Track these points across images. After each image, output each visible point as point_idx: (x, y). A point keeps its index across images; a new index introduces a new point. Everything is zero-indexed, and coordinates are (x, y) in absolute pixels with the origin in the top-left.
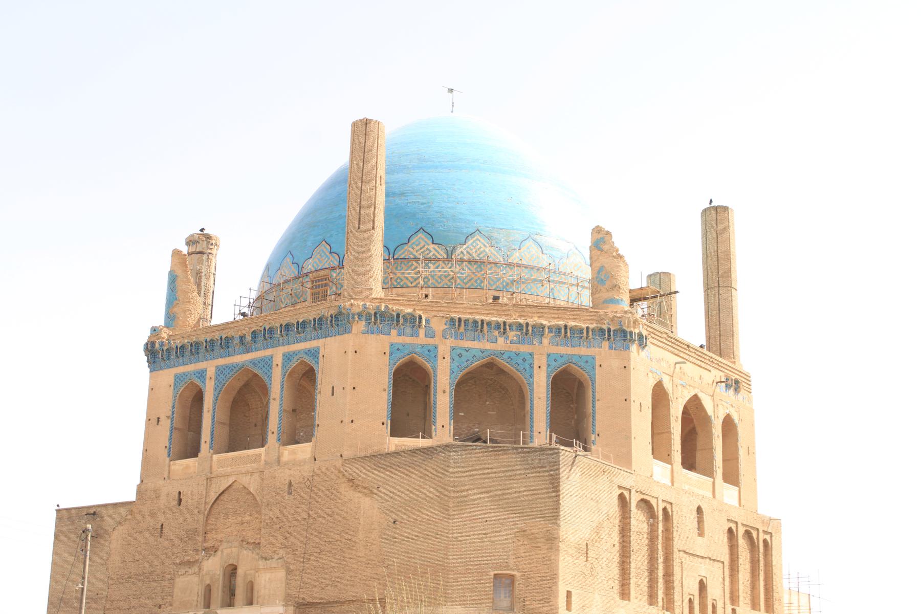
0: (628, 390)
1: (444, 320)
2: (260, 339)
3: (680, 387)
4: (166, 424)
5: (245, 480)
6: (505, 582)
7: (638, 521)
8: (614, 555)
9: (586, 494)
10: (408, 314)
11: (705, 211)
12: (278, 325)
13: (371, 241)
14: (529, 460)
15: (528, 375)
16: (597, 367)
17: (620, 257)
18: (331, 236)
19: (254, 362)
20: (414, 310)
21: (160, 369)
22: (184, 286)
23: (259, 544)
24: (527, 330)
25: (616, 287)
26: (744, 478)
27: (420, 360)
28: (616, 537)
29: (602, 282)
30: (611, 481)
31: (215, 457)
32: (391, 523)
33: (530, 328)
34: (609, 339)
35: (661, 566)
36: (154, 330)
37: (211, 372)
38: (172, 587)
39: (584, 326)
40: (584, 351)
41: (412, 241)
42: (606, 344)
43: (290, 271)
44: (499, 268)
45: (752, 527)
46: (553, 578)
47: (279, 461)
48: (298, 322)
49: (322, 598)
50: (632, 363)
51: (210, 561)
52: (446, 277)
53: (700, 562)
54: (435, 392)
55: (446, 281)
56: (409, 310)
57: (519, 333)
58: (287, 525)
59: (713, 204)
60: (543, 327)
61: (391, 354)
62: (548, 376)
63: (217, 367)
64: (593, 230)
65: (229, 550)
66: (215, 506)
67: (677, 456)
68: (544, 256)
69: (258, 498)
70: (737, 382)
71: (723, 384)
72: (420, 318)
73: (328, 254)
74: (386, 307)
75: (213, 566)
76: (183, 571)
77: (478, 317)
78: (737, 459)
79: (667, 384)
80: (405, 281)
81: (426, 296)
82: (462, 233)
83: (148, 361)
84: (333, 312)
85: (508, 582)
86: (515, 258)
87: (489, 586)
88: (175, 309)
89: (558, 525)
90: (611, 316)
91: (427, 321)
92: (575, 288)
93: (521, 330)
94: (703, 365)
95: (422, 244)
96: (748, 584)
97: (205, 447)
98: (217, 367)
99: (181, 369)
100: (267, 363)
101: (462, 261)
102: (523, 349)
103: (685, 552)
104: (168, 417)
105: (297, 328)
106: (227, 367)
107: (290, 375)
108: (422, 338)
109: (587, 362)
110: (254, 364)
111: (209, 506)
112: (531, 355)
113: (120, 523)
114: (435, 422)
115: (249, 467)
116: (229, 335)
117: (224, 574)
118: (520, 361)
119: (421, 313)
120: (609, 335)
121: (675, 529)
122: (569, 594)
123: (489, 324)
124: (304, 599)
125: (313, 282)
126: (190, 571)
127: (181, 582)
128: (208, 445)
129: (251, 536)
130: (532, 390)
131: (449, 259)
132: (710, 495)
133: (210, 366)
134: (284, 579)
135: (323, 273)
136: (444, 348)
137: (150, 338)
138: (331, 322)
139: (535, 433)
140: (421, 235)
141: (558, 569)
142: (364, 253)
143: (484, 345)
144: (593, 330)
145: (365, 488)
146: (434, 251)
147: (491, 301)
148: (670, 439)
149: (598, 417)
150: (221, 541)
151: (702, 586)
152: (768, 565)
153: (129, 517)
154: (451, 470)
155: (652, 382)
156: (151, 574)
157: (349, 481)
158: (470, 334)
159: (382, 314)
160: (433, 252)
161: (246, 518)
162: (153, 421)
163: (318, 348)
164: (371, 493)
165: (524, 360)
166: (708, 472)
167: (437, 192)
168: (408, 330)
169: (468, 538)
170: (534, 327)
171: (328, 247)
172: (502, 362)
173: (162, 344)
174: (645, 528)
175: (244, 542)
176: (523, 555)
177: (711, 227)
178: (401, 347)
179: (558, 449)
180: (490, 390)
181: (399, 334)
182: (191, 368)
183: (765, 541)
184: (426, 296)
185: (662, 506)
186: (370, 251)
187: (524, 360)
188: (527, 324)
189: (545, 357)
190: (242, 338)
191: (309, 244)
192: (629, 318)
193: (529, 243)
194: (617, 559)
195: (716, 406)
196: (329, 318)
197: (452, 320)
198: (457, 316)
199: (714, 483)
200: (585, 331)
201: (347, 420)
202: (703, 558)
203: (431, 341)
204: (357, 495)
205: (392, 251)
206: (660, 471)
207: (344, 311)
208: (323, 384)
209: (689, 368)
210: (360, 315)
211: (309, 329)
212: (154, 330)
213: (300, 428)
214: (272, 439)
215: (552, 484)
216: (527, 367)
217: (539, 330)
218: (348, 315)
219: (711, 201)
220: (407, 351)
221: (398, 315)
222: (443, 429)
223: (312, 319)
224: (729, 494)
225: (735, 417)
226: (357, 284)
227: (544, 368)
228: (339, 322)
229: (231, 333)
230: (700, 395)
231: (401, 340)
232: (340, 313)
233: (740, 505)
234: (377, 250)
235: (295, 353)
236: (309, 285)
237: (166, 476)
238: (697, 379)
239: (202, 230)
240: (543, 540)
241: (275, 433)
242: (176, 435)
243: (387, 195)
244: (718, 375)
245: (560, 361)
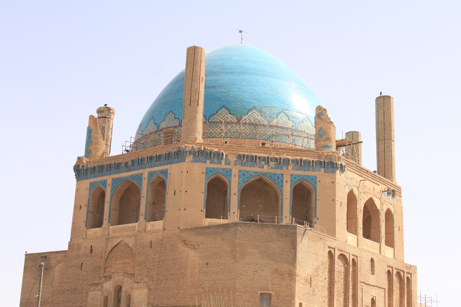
0: (334, 194)
1: (235, 156)
2: (136, 164)
3: (362, 194)
4: (85, 209)
5: (127, 240)
6: (266, 297)
7: (339, 266)
8: (326, 284)
9: (311, 251)
10: (216, 152)
11: (378, 98)
12: (146, 157)
13: (196, 112)
14: (280, 232)
15: (280, 186)
16: (318, 182)
17: (331, 123)
18: (175, 109)
19: (132, 177)
20: (219, 150)
21: (82, 180)
22: (96, 135)
23: (134, 274)
24: (280, 162)
25: (329, 139)
26: (397, 244)
27: (222, 177)
28: (326, 274)
29: (321, 136)
30: (324, 244)
31: (111, 227)
32: (205, 265)
33: (282, 160)
34: (324, 167)
35: (351, 290)
36: (79, 158)
37: (109, 182)
38: (87, 297)
39: (311, 160)
40: (310, 173)
41: (219, 113)
42: (322, 170)
43: (153, 128)
44: (265, 128)
45: (401, 270)
46: (292, 296)
47: (145, 230)
48: (156, 155)
49: (167, 304)
50: (337, 180)
51: (107, 283)
52: (237, 132)
53: (372, 287)
54: (230, 194)
55: (237, 134)
56: (216, 150)
57: (276, 163)
58: (149, 264)
59: (382, 95)
60: (289, 160)
61: (206, 173)
62: (291, 186)
63: (113, 179)
64: (317, 108)
65: (118, 278)
66: (111, 254)
67: (361, 231)
68: (290, 122)
69: (133, 250)
70: (393, 191)
71: (386, 192)
72: (223, 154)
73: (173, 119)
74: (204, 148)
75: (109, 286)
76: (93, 289)
77: (254, 154)
78: (393, 233)
79: (356, 192)
80: (215, 134)
81: (226, 142)
82: (246, 109)
83: (76, 175)
84: (175, 150)
85: (268, 297)
86: (274, 122)
87: (258, 300)
88: (91, 148)
89: (296, 267)
90: (325, 154)
91: (226, 156)
92: (306, 139)
93: (277, 161)
94: (375, 182)
95: (224, 114)
96: (398, 301)
97: (105, 222)
98: (113, 179)
99: (93, 180)
100: (140, 177)
101: (245, 123)
102: (278, 171)
103: (364, 283)
104: (86, 206)
105: (156, 159)
106: (118, 179)
107: (152, 184)
108: (223, 165)
109: (312, 179)
110: (133, 178)
111: (107, 254)
112: (282, 175)
113: (59, 262)
114: (229, 211)
115: (129, 233)
116: (119, 162)
117: (115, 291)
118: (276, 178)
119: (223, 151)
120: (325, 165)
121: (359, 270)
122: (301, 304)
123: (260, 158)
124: (157, 305)
125: (165, 134)
126: (97, 289)
127: (91, 294)
128: (107, 221)
130: (282, 194)
131: (238, 122)
132: (378, 252)
133: (109, 179)
134: (147, 294)
135: (170, 129)
136: (235, 171)
137: (77, 162)
138: (174, 155)
139: (284, 217)
140: (223, 109)
141: (295, 291)
142: (193, 118)
143: (257, 169)
144: (316, 162)
145: (192, 245)
146: (230, 118)
147: (261, 145)
148: (357, 221)
149: (318, 209)
150: (113, 273)
151: (373, 301)
152: (409, 291)
153: (64, 259)
154: (238, 237)
155: (347, 191)
156: (75, 290)
157: (183, 241)
158: (249, 163)
159: (202, 152)
160: (230, 119)
161: (127, 261)
162: (78, 207)
163: (167, 169)
164: (195, 248)
165: (278, 178)
166: (378, 240)
167: (233, 86)
168: (216, 161)
169: (247, 273)
170: (284, 160)
171: (173, 115)
172: (266, 179)
173: (83, 166)
174: (342, 269)
175: (126, 274)
176: (277, 283)
177: (381, 107)
178: (212, 170)
179: (296, 226)
180: (260, 194)
181: (211, 163)
182: (99, 179)
183: (408, 278)
184: (226, 142)
185: (352, 257)
186: (196, 118)
187: (278, 178)
188: (280, 158)
189: (289, 177)
190: (126, 164)
191: (163, 113)
192: (335, 156)
193: (282, 115)
194: (327, 286)
195: (382, 204)
196: (173, 154)
197: (240, 155)
198: (242, 153)
199: (380, 246)
200: (311, 163)
201: (182, 208)
202: (374, 286)
203: (228, 167)
204: (187, 249)
205: (208, 118)
206: (351, 239)
207: (181, 150)
209: (368, 184)
210: (190, 152)
211: (163, 159)
212: (79, 158)
213: (157, 213)
214: (142, 218)
215: (293, 245)
216: (280, 181)
217: (287, 161)
218: (184, 152)
219: (381, 93)
220: (215, 172)
221: (211, 153)
222: (234, 215)
223: (164, 154)
224: (388, 252)
225: (392, 210)
226: (189, 135)
227: (289, 182)
228: (179, 156)
229: (120, 161)
230: (374, 198)
231: (212, 166)
232: (179, 151)
233: (394, 258)
234: (200, 117)
235: (155, 172)
236: (163, 136)
237: (84, 237)
238: (372, 189)
239: (106, 105)
240: (287, 275)
241: (144, 215)
243: (206, 87)
244: (384, 187)
245: (298, 178)
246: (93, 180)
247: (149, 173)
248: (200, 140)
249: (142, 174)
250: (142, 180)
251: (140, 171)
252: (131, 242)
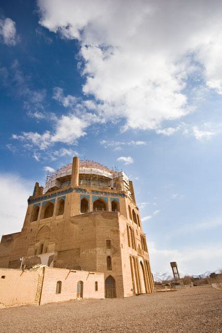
4: (30, 215)
5: (47, 224)
46: (119, 240)
75: (38, 244)
97: (39, 218)
99: (35, 204)
100: (54, 200)
108: (86, 194)
127: (29, 249)
129: (47, 237)
133: (41, 202)
136: (91, 196)
162: (28, 214)
166: (136, 223)
180: (100, 204)
182: (37, 203)
208: (66, 203)
213: (61, 210)
214: (54, 215)
228: (70, 190)
248: (78, 185)
252: (49, 225)
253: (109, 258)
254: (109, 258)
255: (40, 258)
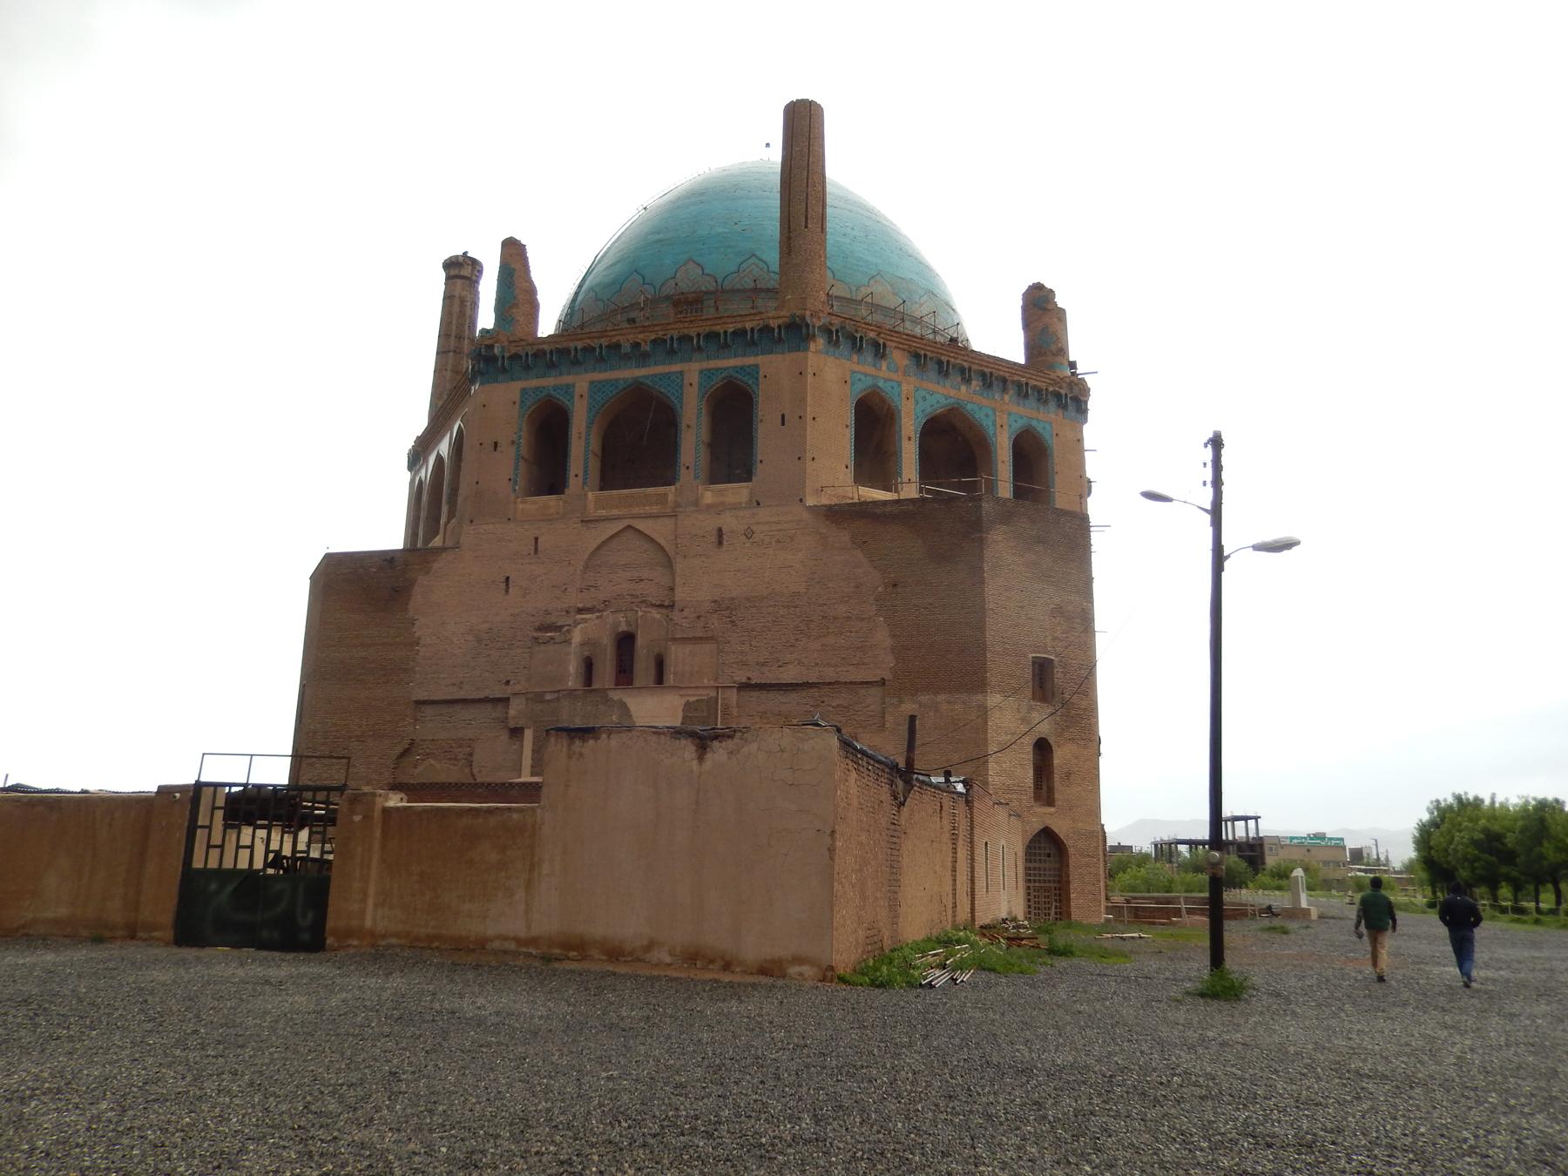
47: (696, 503)
63: (592, 382)
97: (574, 483)
115: (655, 509)
163: (757, 366)
168: (870, 359)
182: (550, 382)
222: (910, 487)
242: (522, 466)
246: (535, 383)
247: (701, 372)
249: (681, 373)
250: (681, 387)
251: (676, 368)
253: (1043, 748)
254: (1043, 748)
255: (624, 706)
